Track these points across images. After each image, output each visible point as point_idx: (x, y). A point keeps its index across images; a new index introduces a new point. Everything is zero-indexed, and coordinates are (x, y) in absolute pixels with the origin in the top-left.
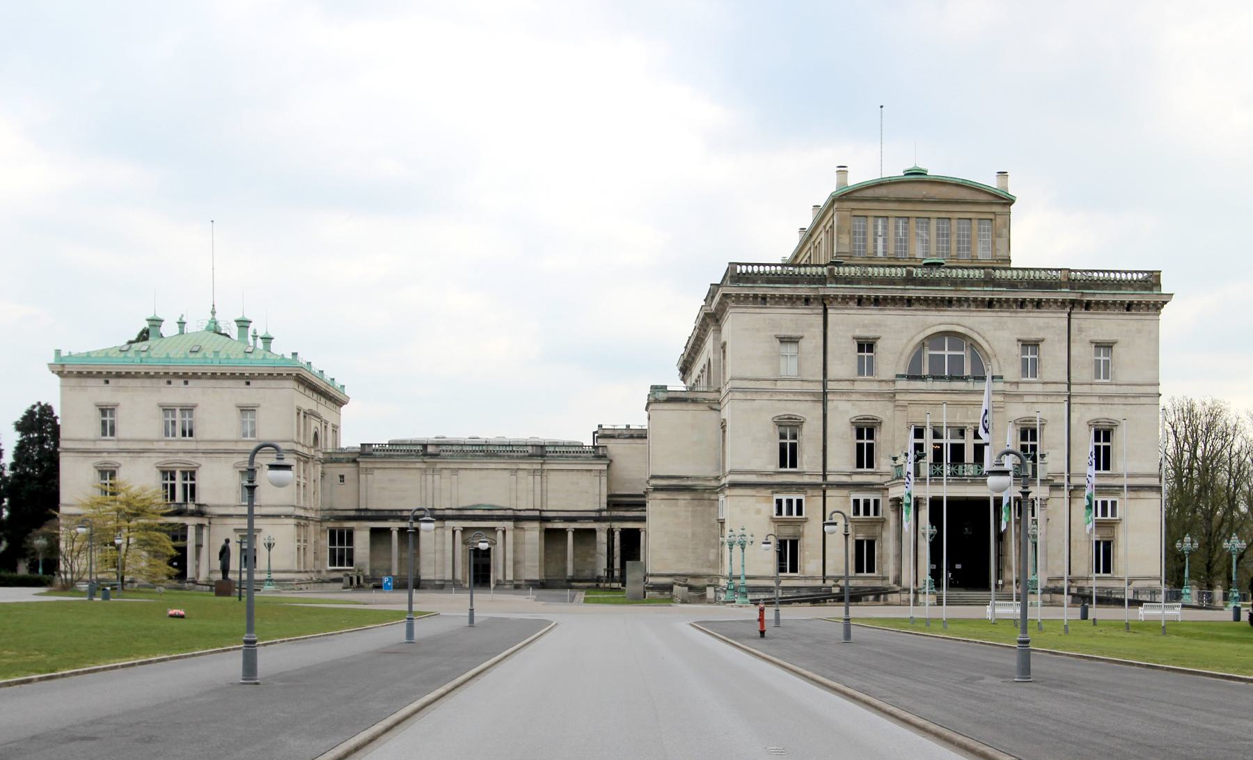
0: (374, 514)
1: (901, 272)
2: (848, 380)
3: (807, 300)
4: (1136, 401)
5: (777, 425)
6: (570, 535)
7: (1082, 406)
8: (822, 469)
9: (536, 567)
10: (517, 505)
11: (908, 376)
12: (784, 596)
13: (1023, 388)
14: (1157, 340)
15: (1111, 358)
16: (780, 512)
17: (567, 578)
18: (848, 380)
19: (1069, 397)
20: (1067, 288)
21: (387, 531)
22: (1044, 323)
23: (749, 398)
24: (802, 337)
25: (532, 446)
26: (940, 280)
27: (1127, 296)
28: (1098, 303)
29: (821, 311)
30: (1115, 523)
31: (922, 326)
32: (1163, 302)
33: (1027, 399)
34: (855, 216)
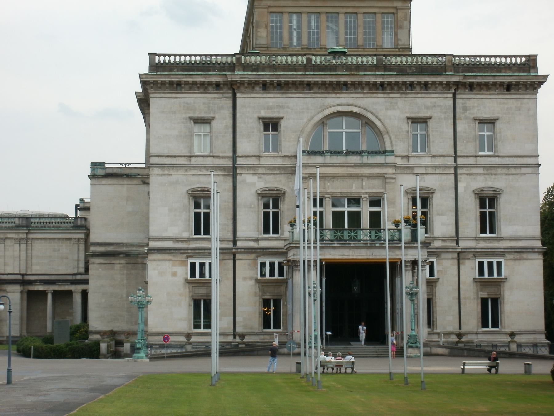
1: (302, 60)
2: (255, 156)
3: (218, 86)
4: (518, 171)
5: (191, 196)
6: (50, 297)
7: (468, 176)
8: (232, 235)
10: (4, 271)
11: (308, 151)
12: (194, 350)
13: (413, 161)
14: (535, 117)
15: (494, 133)
16: (193, 274)
18: (255, 156)
19: (456, 168)
20: (451, 71)
22: (431, 103)
23: (166, 172)
24: (213, 119)
25: (19, 218)
26: (336, 66)
27: (506, 78)
28: (479, 84)
29: (230, 95)
30: (501, 282)
31: (321, 107)
32: (539, 82)
33: (417, 171)
34: (271, 12)
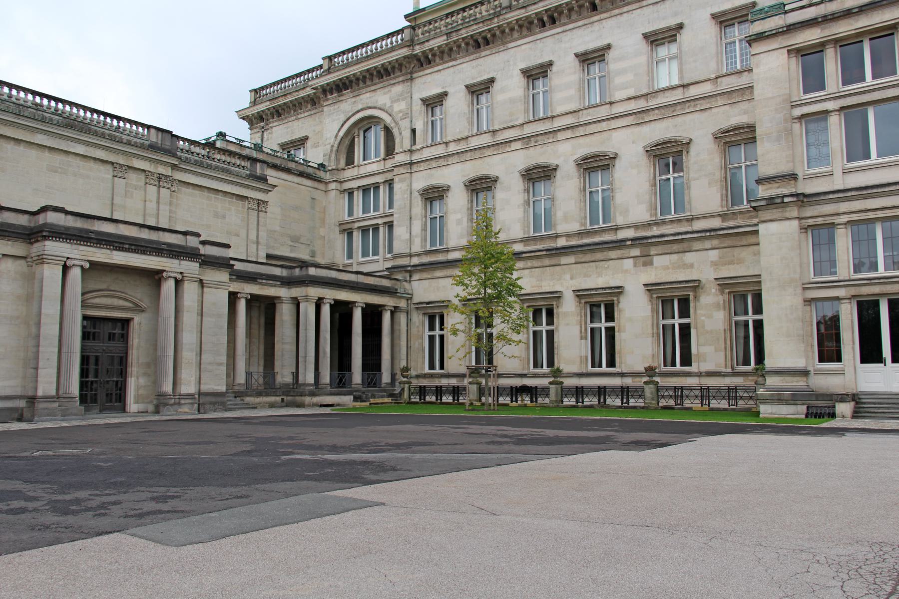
9: (221, 364)
17: (236, 388)
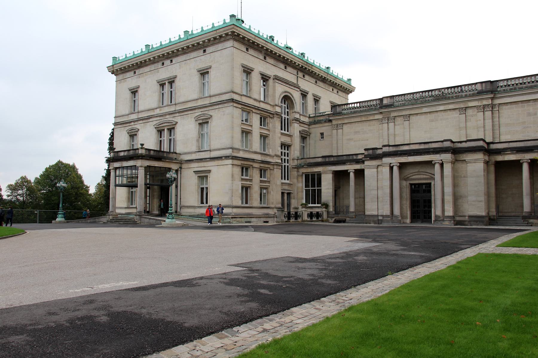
0: (335, 159)
6: (525, 168)
9: (481, 201)
21: (346, 173)
